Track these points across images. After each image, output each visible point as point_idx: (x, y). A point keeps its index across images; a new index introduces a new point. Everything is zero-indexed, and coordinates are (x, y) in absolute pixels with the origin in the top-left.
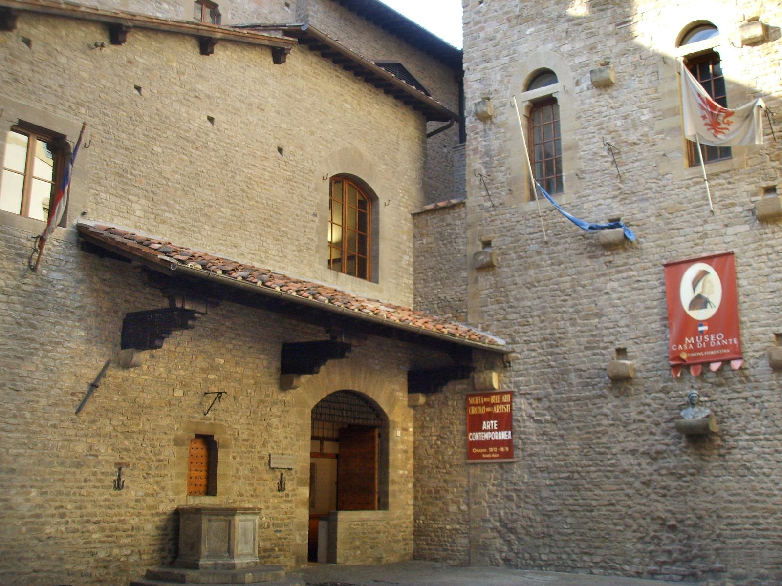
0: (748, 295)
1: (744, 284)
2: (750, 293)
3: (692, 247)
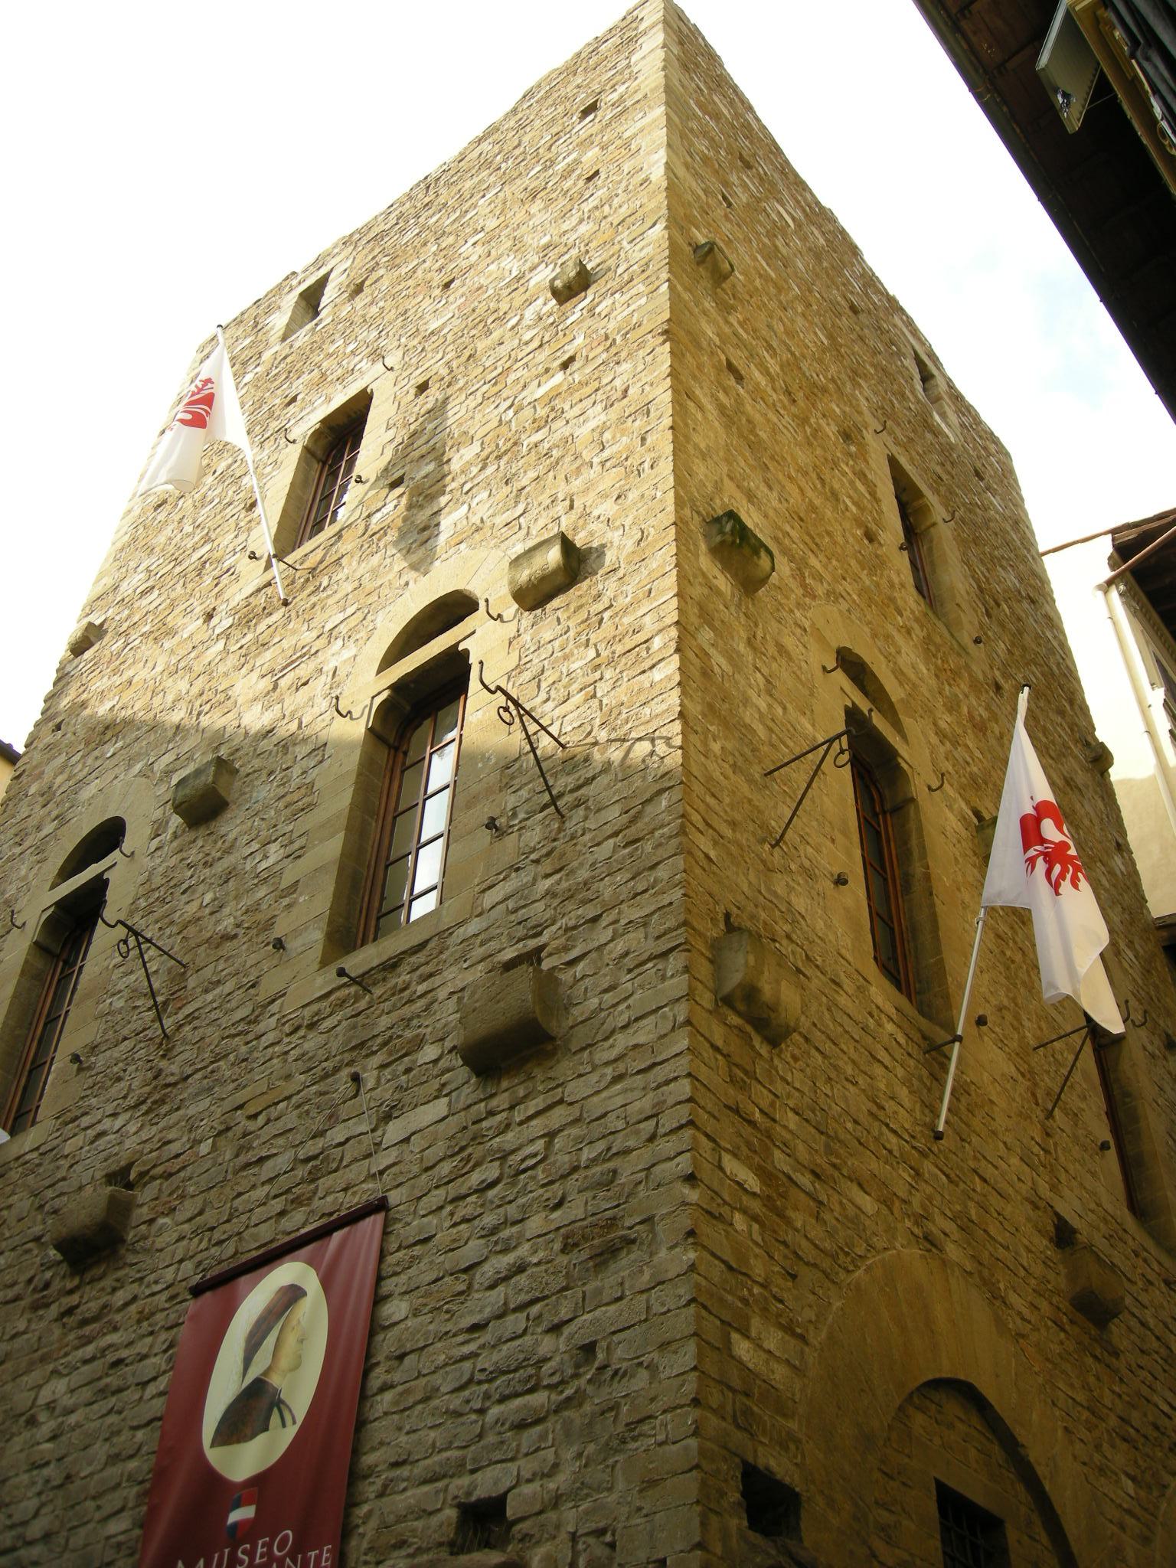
0: (401, 1357)
1: (396, 1318)
2: (409, 1347)
3: (282, 1214)
